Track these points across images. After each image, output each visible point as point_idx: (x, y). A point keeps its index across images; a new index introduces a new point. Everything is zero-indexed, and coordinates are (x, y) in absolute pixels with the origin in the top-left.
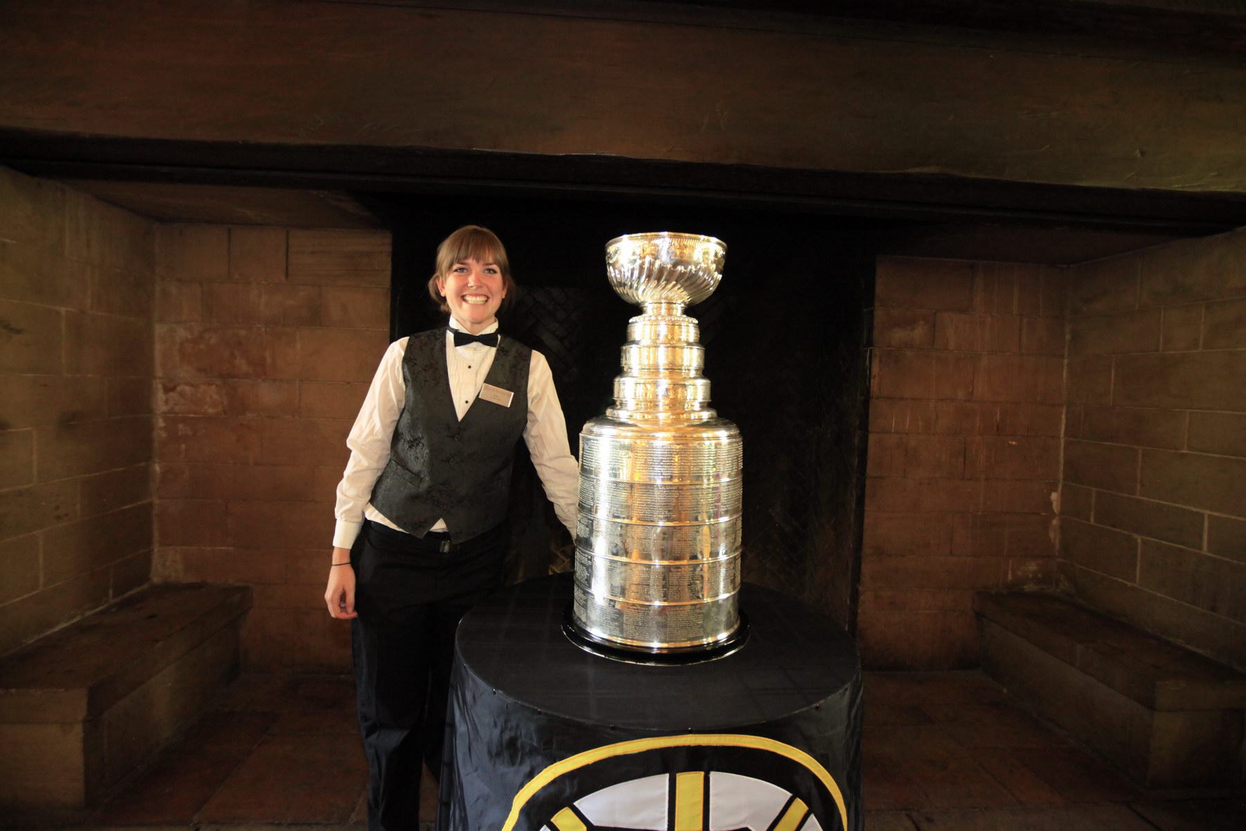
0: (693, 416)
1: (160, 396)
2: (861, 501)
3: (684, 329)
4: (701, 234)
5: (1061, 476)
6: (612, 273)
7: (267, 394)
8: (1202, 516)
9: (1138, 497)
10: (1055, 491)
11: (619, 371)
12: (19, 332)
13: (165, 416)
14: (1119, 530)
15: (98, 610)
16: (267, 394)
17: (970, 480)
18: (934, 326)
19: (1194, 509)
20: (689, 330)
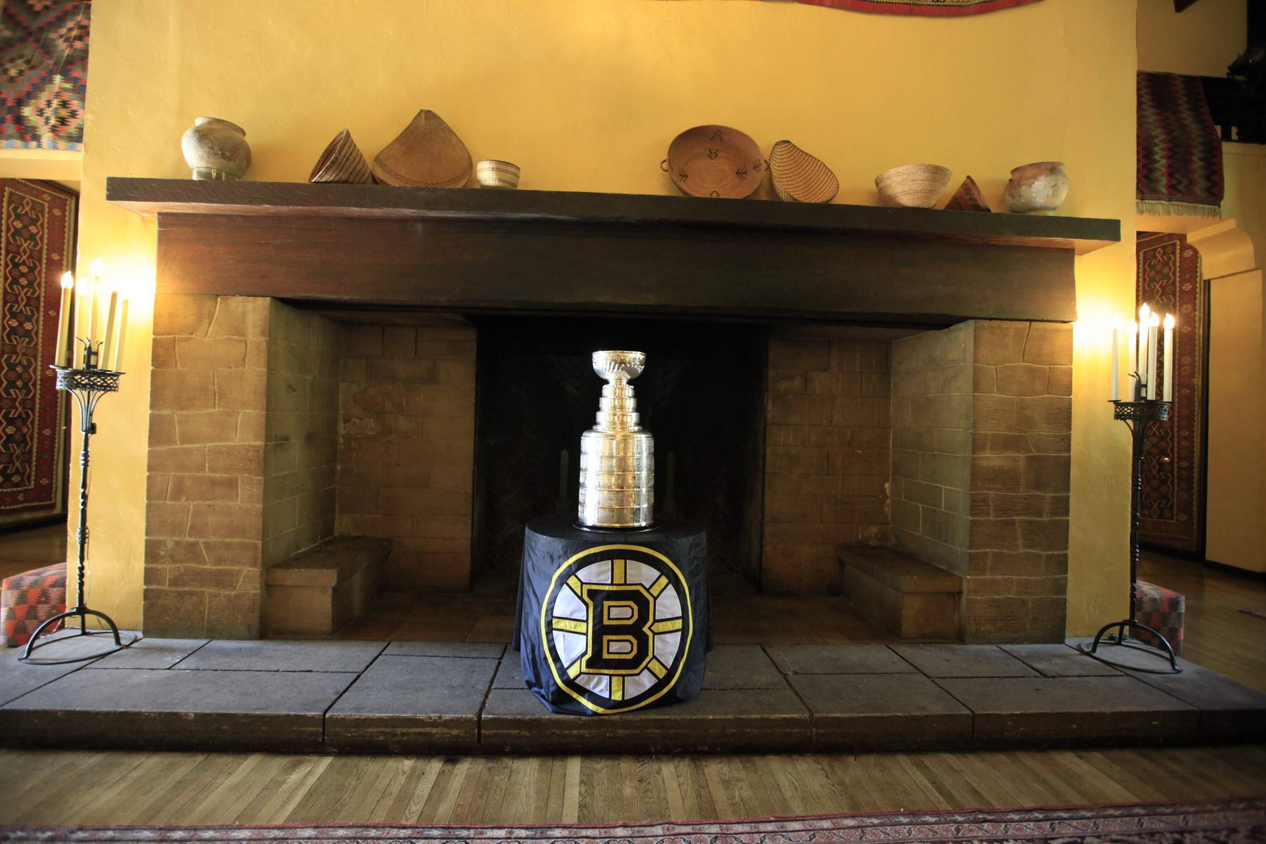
0: (630, 428)
1: (342, 425)
2: (763, 490)
3: (627, 391)
4: (632, 350)
5: (891, 472)
6: (595, 367)
7: (403, 424)
8: (941, 488)
9: (920, 481)
10: (888, 482)
11: (598, 409)
12: (294, 390)
13: (344, 436)
14: (912, 503)
15: (314, 545)
16: (403, 424)
17: (832, 475)
18: (806, 380)
19: (939, 485)
20: (629, 391)
